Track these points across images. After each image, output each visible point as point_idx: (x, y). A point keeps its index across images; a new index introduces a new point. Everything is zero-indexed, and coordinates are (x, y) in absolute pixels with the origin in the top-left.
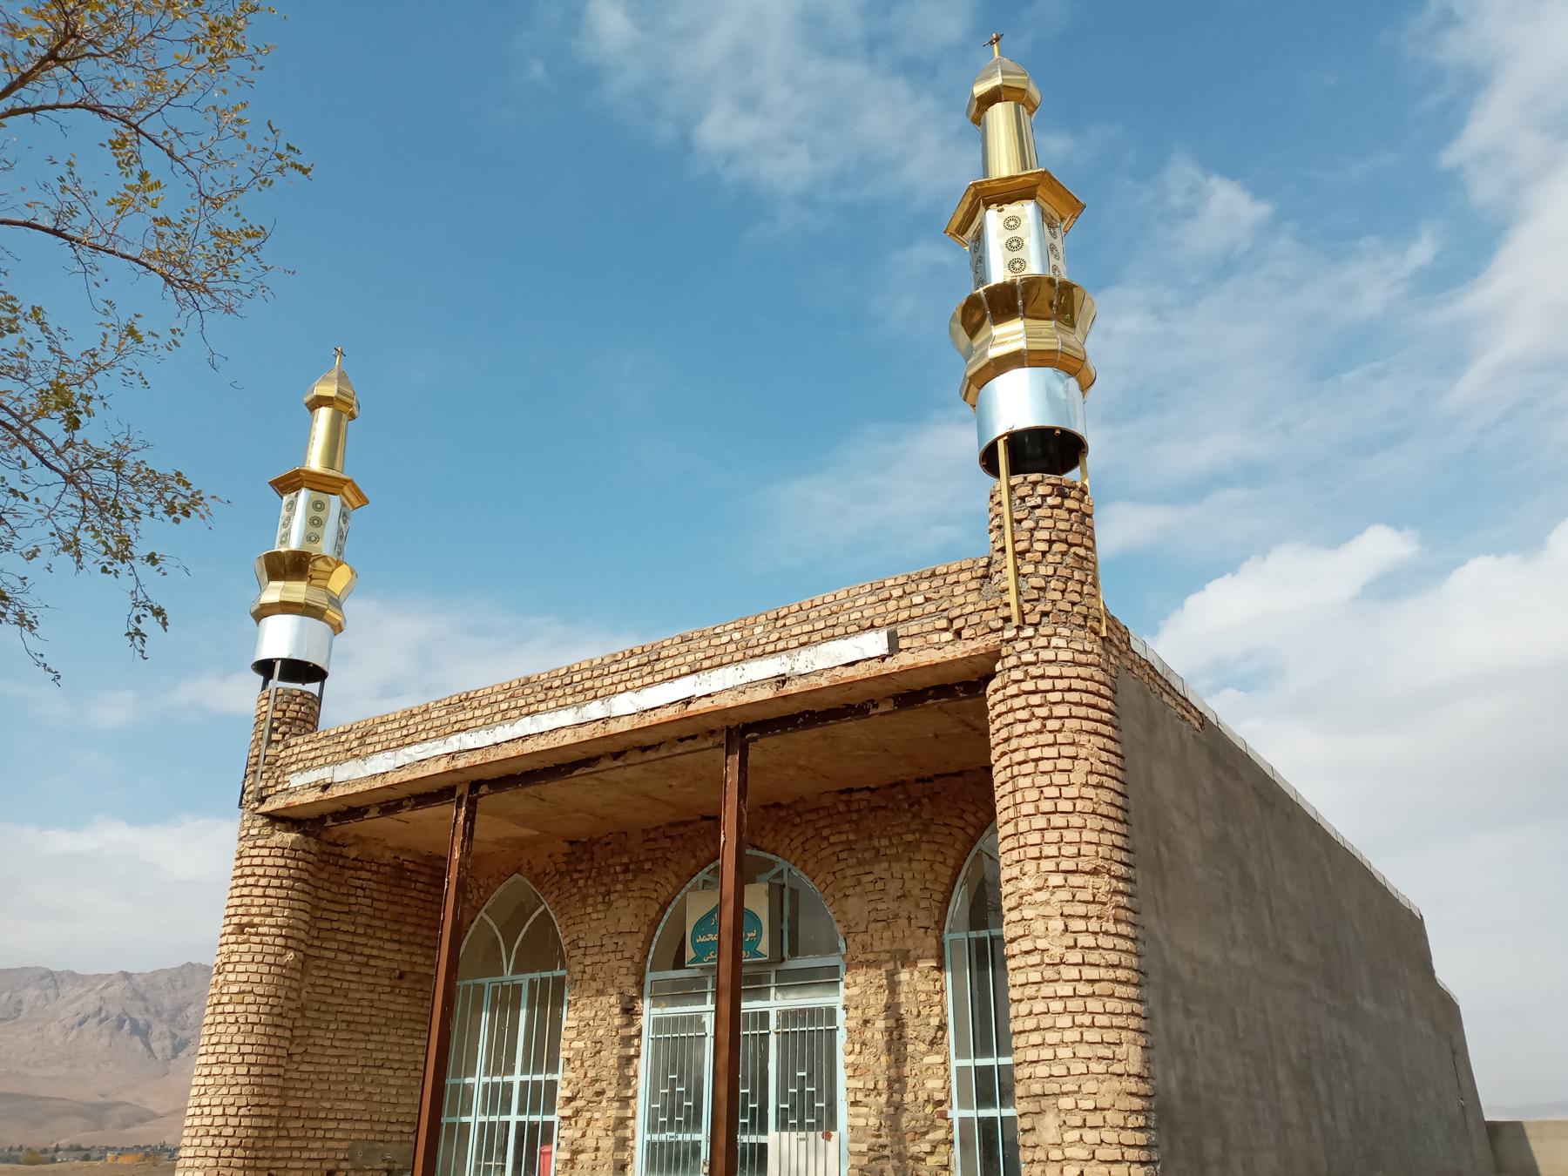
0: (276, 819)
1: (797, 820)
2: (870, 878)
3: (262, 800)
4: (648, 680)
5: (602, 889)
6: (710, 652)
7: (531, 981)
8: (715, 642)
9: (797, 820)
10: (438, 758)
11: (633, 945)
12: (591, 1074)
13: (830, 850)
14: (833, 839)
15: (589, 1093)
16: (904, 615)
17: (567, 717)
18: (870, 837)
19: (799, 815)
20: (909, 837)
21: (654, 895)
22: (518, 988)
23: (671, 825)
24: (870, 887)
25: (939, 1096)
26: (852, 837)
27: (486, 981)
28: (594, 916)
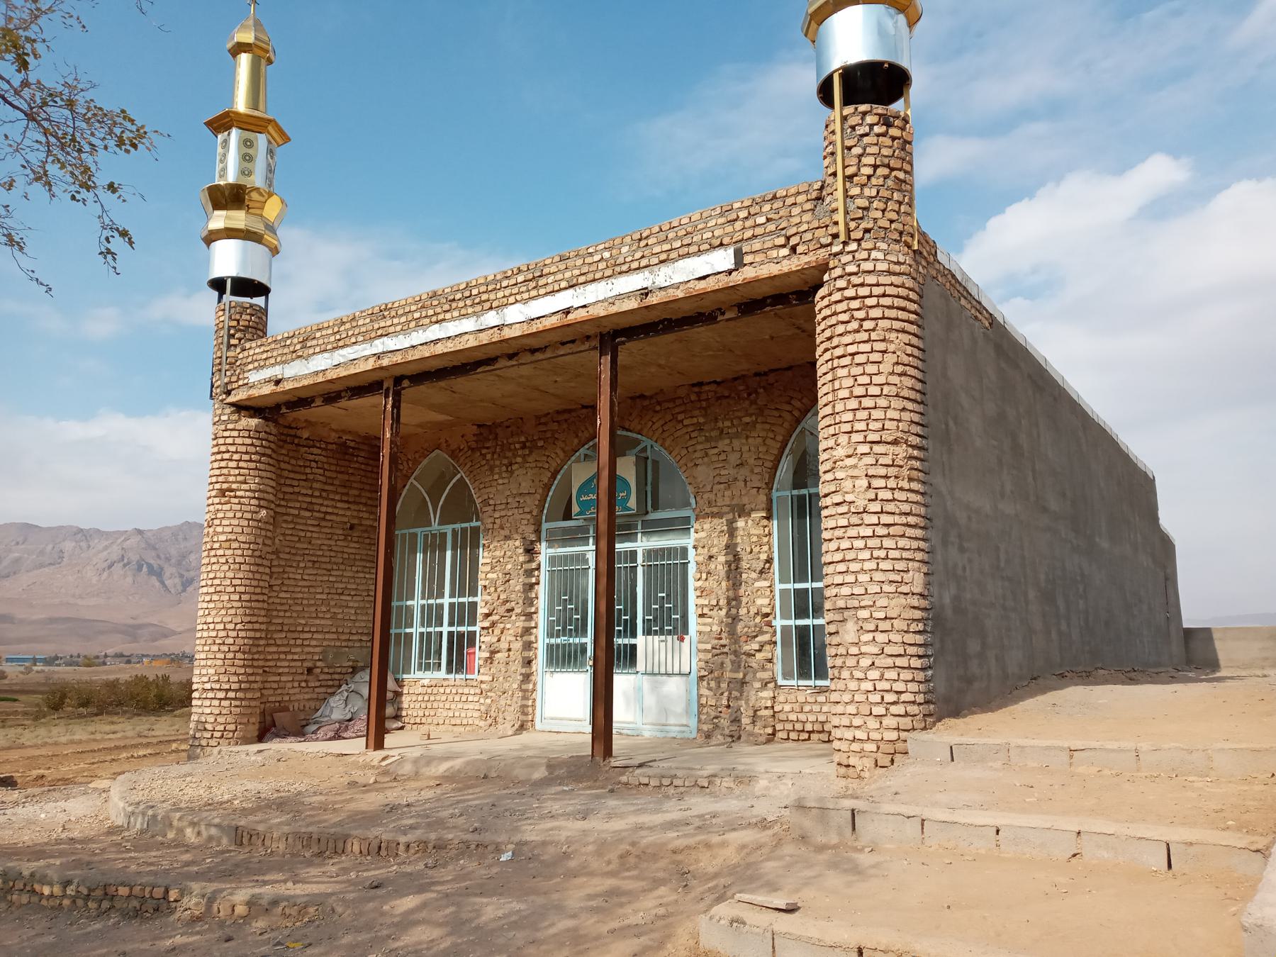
0: (241, 408)
1: (658, 408)
2: (715, 451)
3: (228, 393)
4: (534, 293)
5: (505, 461)
6: (585, 270)
7: (454, 530)
8: (589, 260)
9: (658, 408)
10: (367, 358)
11: (531, 503)
12: (503, 596)
13: (685, 430)
14: (686, 422)
15: (502, 610)
16: (748, 234)
17: (468, 325)
18: (716, 420)
19: (659, 403)
20: (747, 419)
21: (546, 466)
22: (444, 535)
23: (558, 412)
24: (714, 458)
25: (768, 610)
26: (701, 420)
27: (418, 530)
28: (500, 481)
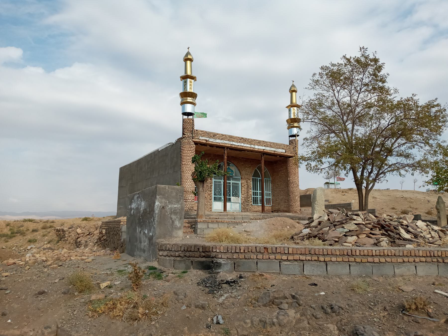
17: (249, 146)
